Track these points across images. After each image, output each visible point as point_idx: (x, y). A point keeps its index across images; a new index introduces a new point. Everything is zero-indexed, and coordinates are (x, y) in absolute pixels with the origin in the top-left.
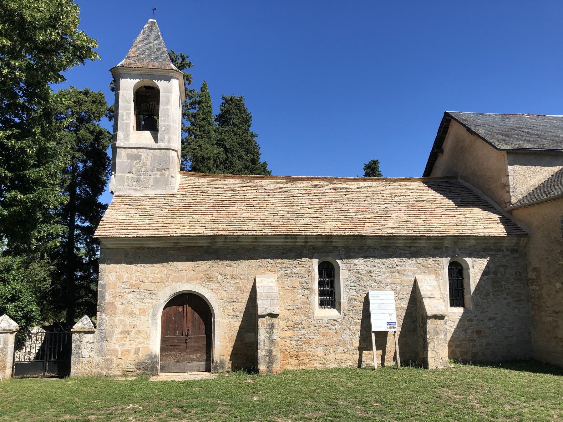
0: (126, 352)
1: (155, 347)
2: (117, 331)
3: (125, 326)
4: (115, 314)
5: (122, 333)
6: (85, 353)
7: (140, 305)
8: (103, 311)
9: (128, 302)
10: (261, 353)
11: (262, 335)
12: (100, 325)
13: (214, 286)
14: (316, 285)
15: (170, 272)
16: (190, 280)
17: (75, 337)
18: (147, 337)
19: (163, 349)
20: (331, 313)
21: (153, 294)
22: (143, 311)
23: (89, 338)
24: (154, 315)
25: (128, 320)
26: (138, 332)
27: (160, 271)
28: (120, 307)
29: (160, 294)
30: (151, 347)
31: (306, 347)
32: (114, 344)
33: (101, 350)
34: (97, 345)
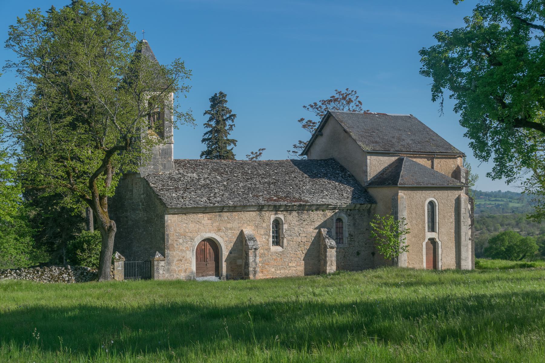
1: (194, 268)
3: (179, 256)
4: (174, 250)
5: (178, 260)
6: (161, 272)
8: (168, 249)
9: (180, 244)
10: (251, 269)
11: (251, 259)
12: (167, 257)
13: (222, 234)
14: (271, 234)
15: (200, 227)
16: (210, 232)
17: (156, 263)
18: (191, 263)
19: (196, 270)
20: (279, 249)
21: (192, 239)
23: (162, 263)
24: (193, 251)
27: (195, 226)
29: (196, 239)
30: (192, 268)
32: (174, 267)
33: (168, 269)
34: (166, 267)
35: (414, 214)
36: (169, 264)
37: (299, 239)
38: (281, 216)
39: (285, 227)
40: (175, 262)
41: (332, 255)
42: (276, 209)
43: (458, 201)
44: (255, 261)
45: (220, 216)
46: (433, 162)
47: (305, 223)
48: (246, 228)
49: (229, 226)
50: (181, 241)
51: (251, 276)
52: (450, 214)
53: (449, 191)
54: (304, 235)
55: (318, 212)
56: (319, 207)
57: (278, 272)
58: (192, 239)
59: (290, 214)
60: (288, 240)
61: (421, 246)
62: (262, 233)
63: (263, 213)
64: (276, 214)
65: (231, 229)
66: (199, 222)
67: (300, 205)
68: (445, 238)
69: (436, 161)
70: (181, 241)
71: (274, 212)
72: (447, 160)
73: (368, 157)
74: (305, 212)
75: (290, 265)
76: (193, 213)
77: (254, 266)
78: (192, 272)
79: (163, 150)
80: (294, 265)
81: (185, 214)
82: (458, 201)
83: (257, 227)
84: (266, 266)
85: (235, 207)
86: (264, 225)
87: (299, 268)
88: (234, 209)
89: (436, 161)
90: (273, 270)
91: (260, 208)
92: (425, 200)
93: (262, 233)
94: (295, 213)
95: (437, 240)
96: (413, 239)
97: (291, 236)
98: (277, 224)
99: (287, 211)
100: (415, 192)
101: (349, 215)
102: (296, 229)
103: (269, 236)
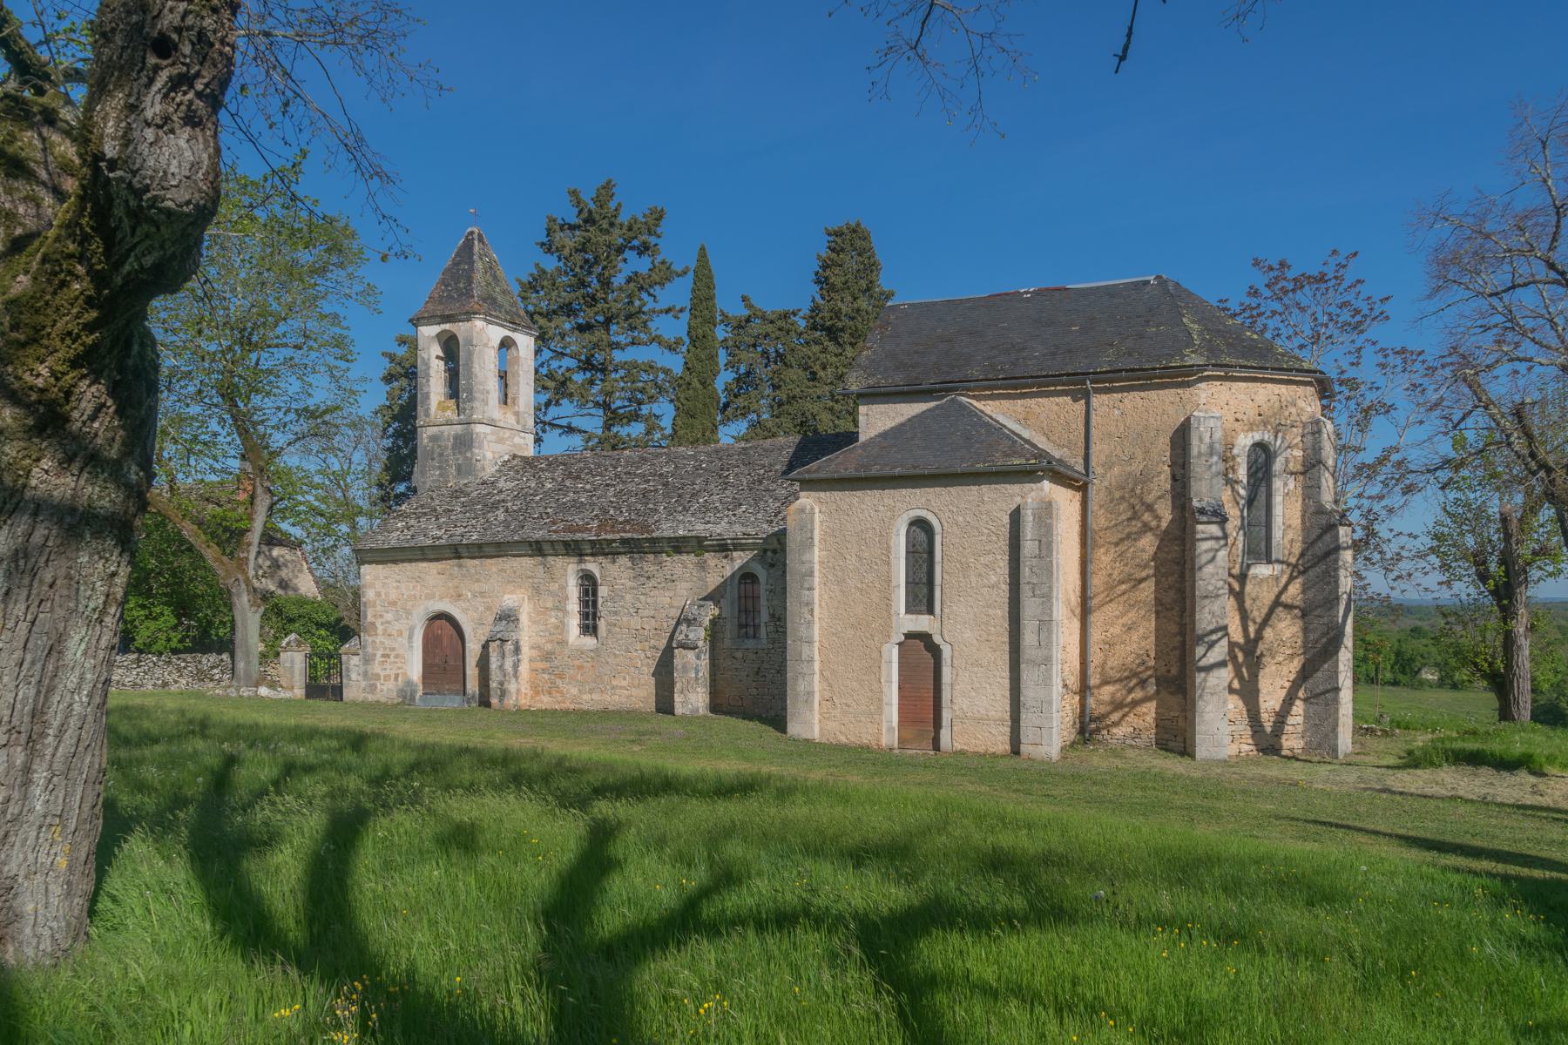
0: (387, 678)
2: (379, 653)
6: (354, 676)
7: (397, 626)
17: (344, 658)
20: (590, 642)
22: (400, 633)
23: (355, 660)
24: (410, 637)
25: (387, 642)
26: (397, 656)
28: (380, 628)
31: (559, 682)
34: (362, 668)
35: (852, 561)
36: (368, 660)
37: (636, 622)
38: (592, 566)
39: (603, 591)
40: (379, 658)
41: (693, 667)
42: (574, 549)
43: (1016, 516)
44: (501, 667)
45: (460, 566)
46: (1088, 404)
47: (653, 582)
48: (512, 592)
49: (476, 587)
50: (389, 617)
51: (494, 701)
52: (991, 558)
53: (985, 488)
54: (646, 613)
55: (684, 557)
56: (678, 546)
57: (586, 697)
58: (408, 613)
59: (614, 562)
60: (609, 624)
61: (875, 655)
62: (549, 605)
63: (550, 559)
64: (580, 562)
65: (482, 594)
66: (419, 579)
67: (624, 541)
68: (968, 634)
69: (1096, 400)
70: (389, 617)
71: (576, 559)
72: (1153, 394)
73: (862, 409)
74: (651, 557)
75: (615, 683)
76: (410, 561)
77: (500, 678)
78: (409, 683)
79: (456, 437)
80: (624, 683)
81: (395, 562)
82: (1016, 516)
83: (537, 591)
84: (559, 682)
85: (480, 546)
86: (554, 587)
87: (634, 691)
88: (479, 551)
89: (1096, 400)
90: (574, 691)
91: (537, 549)
92: (893, 517)
93: (549, 605)
94: (624, 560)
95: (937, 639)
96: (850, 632)
97: (616, 613)
98: (589, 586)
99: (605, 554)
100: (859, 493)
101: (772, 565)
102: (628, 597)
103: (565, 612)
